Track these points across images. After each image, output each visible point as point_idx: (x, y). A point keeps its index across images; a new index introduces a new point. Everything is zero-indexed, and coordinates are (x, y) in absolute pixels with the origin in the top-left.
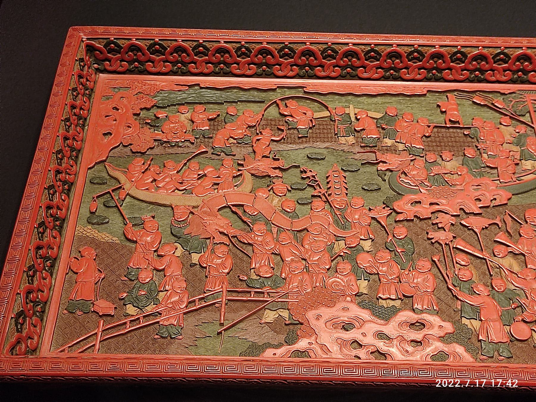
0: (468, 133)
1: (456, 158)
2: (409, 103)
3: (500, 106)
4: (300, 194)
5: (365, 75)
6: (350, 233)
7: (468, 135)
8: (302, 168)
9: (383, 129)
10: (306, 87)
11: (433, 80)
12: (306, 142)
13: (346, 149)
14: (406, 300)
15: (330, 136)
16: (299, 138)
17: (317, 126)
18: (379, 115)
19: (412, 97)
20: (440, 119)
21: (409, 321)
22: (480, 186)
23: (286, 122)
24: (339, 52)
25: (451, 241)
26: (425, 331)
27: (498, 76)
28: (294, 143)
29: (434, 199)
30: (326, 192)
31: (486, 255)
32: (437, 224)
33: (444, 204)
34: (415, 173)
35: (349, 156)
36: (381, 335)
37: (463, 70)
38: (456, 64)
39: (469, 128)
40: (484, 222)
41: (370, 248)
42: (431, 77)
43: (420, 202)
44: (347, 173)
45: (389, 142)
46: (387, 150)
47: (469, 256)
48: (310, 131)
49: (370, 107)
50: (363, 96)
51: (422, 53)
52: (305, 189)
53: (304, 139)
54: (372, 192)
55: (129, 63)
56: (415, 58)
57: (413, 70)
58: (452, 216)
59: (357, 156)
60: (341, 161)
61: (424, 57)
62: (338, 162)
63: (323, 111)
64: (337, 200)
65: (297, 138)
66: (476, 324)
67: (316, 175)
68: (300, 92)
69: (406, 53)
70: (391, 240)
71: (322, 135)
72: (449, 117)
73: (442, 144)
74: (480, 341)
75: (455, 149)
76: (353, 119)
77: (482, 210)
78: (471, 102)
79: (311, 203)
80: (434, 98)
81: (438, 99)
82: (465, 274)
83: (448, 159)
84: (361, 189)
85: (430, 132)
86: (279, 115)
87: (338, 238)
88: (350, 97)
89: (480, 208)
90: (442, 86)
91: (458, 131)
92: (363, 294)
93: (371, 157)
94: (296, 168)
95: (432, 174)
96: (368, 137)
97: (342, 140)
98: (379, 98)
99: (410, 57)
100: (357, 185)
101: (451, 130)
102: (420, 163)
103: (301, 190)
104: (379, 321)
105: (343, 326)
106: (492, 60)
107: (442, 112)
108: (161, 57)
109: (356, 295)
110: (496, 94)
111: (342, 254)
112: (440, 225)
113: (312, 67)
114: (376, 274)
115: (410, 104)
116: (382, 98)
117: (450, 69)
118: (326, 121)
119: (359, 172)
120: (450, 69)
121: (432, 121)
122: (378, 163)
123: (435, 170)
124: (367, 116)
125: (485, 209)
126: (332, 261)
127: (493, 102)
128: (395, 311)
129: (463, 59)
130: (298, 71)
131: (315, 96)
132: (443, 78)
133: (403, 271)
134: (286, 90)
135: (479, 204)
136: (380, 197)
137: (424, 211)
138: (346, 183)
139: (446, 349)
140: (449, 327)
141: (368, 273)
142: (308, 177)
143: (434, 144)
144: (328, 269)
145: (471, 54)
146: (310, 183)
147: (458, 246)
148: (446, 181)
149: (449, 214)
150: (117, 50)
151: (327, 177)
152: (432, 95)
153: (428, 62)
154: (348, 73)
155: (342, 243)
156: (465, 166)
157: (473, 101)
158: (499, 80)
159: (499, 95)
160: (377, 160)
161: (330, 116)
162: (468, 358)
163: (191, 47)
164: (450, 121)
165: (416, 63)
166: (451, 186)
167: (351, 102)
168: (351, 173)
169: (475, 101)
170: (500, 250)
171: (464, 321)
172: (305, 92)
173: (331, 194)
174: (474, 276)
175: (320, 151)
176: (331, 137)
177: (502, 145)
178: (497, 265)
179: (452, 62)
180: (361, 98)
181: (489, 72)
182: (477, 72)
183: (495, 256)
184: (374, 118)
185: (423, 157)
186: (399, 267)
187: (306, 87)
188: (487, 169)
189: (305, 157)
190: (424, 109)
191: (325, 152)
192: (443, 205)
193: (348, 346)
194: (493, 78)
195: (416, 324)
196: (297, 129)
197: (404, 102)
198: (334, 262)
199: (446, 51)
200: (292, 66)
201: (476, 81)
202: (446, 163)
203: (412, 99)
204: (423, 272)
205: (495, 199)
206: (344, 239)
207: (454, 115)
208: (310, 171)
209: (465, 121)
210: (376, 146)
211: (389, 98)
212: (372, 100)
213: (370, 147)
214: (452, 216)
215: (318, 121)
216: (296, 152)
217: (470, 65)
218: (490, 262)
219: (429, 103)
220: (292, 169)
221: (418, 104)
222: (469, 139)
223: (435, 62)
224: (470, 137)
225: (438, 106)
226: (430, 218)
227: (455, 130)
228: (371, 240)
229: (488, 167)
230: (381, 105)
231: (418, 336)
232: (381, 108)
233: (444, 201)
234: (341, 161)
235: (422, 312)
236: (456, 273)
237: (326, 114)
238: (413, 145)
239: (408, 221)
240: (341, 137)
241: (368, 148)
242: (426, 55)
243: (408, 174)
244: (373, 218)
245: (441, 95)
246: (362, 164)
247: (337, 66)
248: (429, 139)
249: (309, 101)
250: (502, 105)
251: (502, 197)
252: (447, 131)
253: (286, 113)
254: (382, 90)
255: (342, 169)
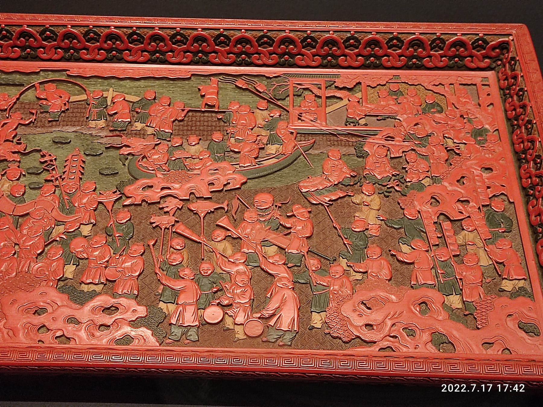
0: (221, 117)
1: (204, 142)
2: (171, 87)
3: (260, 90)
4: (34, 179)
5: (130, 58)
6: (71, 218)
7: (221, 119)
8: (44, 151)
9: (137, 113)
10: (69, 70)
11: (200, 63)
12: (56, 125)
13: (94, 133)
14: (110, 285)
15: (82, 119)
16: (50, 121)
17: (71, 110)
18: (135, 99)
19: (175, 81)
20: (198, 104)
21: (103, 305)
22: (218, 170)
23: (40, 106)
24: (102, 35)
25: (173, 225)
26: (118, 316)
27: (264, 59)
28: (43, 126)
29: (167, 183)
30: (61, 177)
31: (202, 239)
32: (163, 208)
33: (177, 188)
34: (156, 157)
35: (94, 140)
36: (73, 319)
37: (228, 54)
38: (221, 47)
39: (224, 112)
40: (210, 206)
41: (88, 233)
42: (326, 64)
43: (152, 187)
44: (89, 158)
45: (139, 126)
46: (136, 134)
47: (187, 240)
48: (63, 114)
49: (131, 90)
50: (126, 80)
51: (185, 36)
52: (40, 173)
53: (54, 123)
54: (108, 176)
55: (107, 51)
56: (351, 45)
57: (93, 50)
58: (181, 200)
59: (104, 141)
60: (87, 145)
61: (187, 40)
62: (83, 146)
63: (82, 94)
64: (70, 184)
65: (47, 122)
66: (172, 307)
67: (55, 159)
68: (64, 75)
69: (169, 36)
70: (111, 224)
71: (74, 119)
72: (205, 100)
73: (194, 128)
74: (171, 324)
75: (205, 133)
76: (109, 103)
77: (213, 194)
78: (234, 86)
79: (42, 187)
80: (198, 81)
81: (202, 83)
82: (176, 259)
83: (194, 143)
84: (98, 174)
85: (183, 116)
86: (35, 98)
87: (58, 223)
88: (113, 81)
89: (211, 192)
90: (176, 69)
91: (214, 115)
92: (67, 279)
93: (117, 141)
94: (38, 152)
95: (173, 159)
96: (120, 120)
97: (92, 124)
98: (143, 81)
99: (174, 40)
100: (96, 169)
101: (206, 114)
102: (163, 147)
103: (36, 175)
104: (73, 305)
105: (36, 311)
106: (386, 45)
107: (203, 96)
108: (140, 46)
109: (59, 280)
110: (261, 78)
111: (58, 239)
112: (166, 210)
113: (77, 50)
114: (87, 259)
115: (172, 88)
116: (145, 81)
117: (430, 56)
118: (82, 104)
119: (102, 156)
120: (430, 56)
121: (190, 105)
122: (121, 147)
123: (178, 154)
124: (124, 99)
125: (217, 194)
126: (46, 246)
127: (255, 86)
128: (93, 295)
129: (314, 44)
130: (63, 54)
131: (78, 79)
132: (209, 61)
133: (114, 255)
134: (50, 73)
135: (211, 188)
136: (115, 180)
137: (154, 195)
138: (83, 168)
139: (133, 334)
140: (142, 311)
141: (78, 258)
142: (46, 162)
143: (186, 128)
144: (39, 254)
145: (234, 37)
146: (46, 168)
147: (178, 231)
148: (185, 165)
149: (177, 198)
150: (96, 38)
151: (66, 161)
152: (196, 79)
153: (192, 46)
154: (114, 56)
155: (61, 228)
156: (209, 150)
157: (236, 86)
158: (266, 63)
159: (265, 78)
160: (122, 144)
161: (86, 100)
162: (152, 341)
163: (169, 36)
164: (206, 104)
165: (94, 44)
166: (189, 170)
167: (113, 86)
168: (93, 157)
169: (237, 84)
170: (220, 234)
171: (162, 305)
172: (68, 75)
173: (64, 178)
174: (185, 260)
175: (68, 135)
176: (82, 121)
177: (252, 129)
178: (210, 249)
179: (217, 45)
180: (125, 81)
181: (468, 58)
182: (456, 59)
183: (213, 240)
184: (131, 102)
185: (170, 141)
186: (112, 251)
187: (69, 70)
188: (232, 153)
189: (50, 141)
190: (185, 92)
191: (73, 135)
192: (175, 189)
193: (35, 330)
194: (260, 62)
195: (111, 309)
196: (49, 113)
197: (167, 86)
198: (49, 247)
199: (208, 34)
200: (56, 49)
201: (286, 65)
202: (190, 147)
203: (175, 82)
204: (133, 257)
205: (229, 183)
206: (64, 223)
207: (211, 98)
208: (50, 155)
209: (223, 105)
210: (125, 130)
211: (153, 81)
212: (135, 84)
213: (119, 131)
214: (181, 200)
215: (74, 104)
216: (43, 136)
217: (450, 52)
218: (205, 246)
219: (192, 86)
220: (34, 153)
221: (180, 87)
222: (222, 123)
223: (373, 49)
224: (223, 121)
225: (199, 90)
226: (159, 203)
227: (210, 115)
228: (92, 225)
229: (231, 151)
230: (142, 89)
231: (108, 320)
232: (142, 91)
233: (177, 186)
234: (87, 145)
235: (121, 296)
236: (168, 257)
237: (84, 97)
238: (162, 130)
239: (136, 205)
240: (92, 121)
241: (117, 132)
242: (189, 38)
243: (148, 158)
244: (100, 203)
245: (207, 78)
246: (106, 148)
247: (188, 52)
248: (182, 123)
249: (70, 85)
250: (262, 89)
251: (236, 180)
252: (202, 115)
253: (42, 97)
254: (146, 73)
255: (85, 154)
